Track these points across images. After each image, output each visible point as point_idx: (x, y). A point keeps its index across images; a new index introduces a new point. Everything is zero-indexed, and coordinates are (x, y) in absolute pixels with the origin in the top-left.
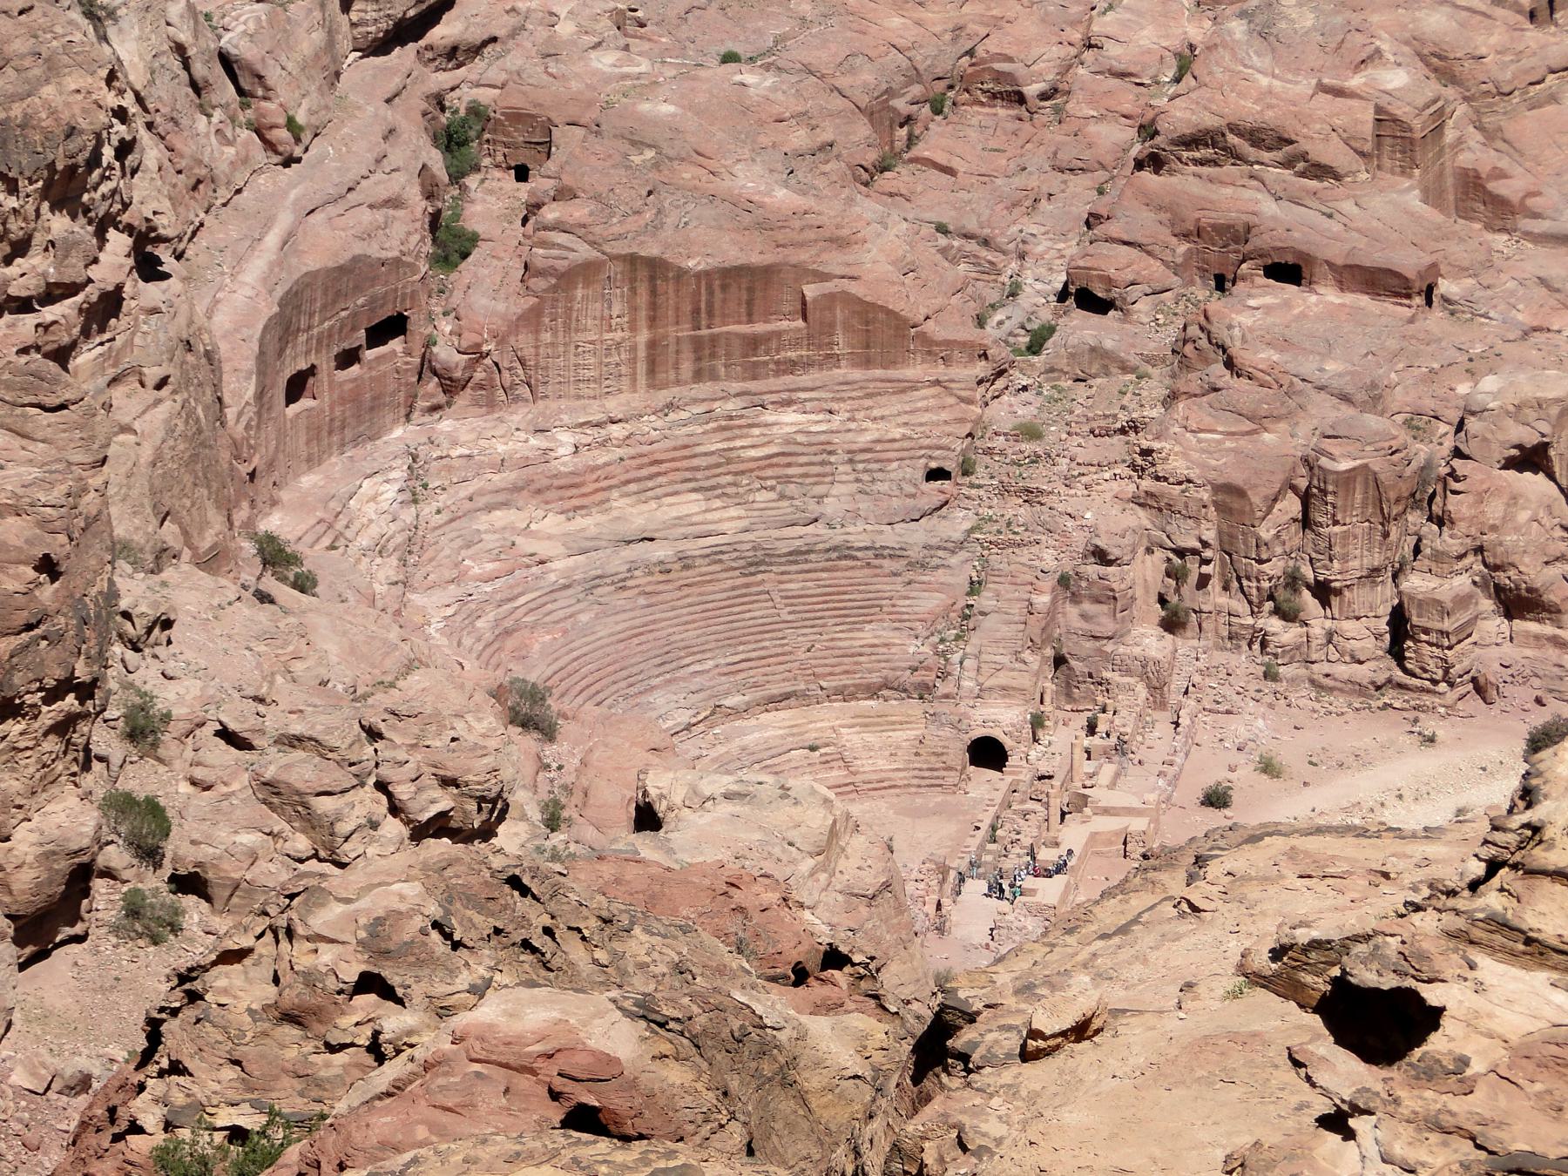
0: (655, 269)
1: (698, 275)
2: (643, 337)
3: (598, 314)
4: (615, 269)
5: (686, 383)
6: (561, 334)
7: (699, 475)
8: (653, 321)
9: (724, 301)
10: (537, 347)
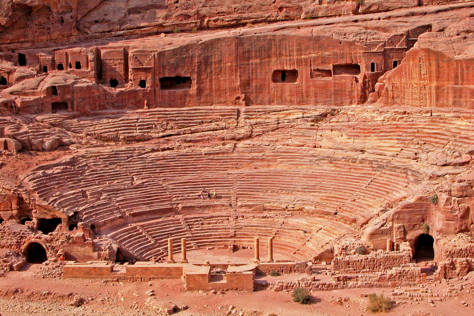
0: (439, 56)
1: (458, 61)
2: (434, 84)
3: (417, 72)
4: (422, 54)
5: (450, 106)
6: (408, 79)
7: (404, 135)
8: (438, 78)
9: (468, 74)
10: (401, 83)
